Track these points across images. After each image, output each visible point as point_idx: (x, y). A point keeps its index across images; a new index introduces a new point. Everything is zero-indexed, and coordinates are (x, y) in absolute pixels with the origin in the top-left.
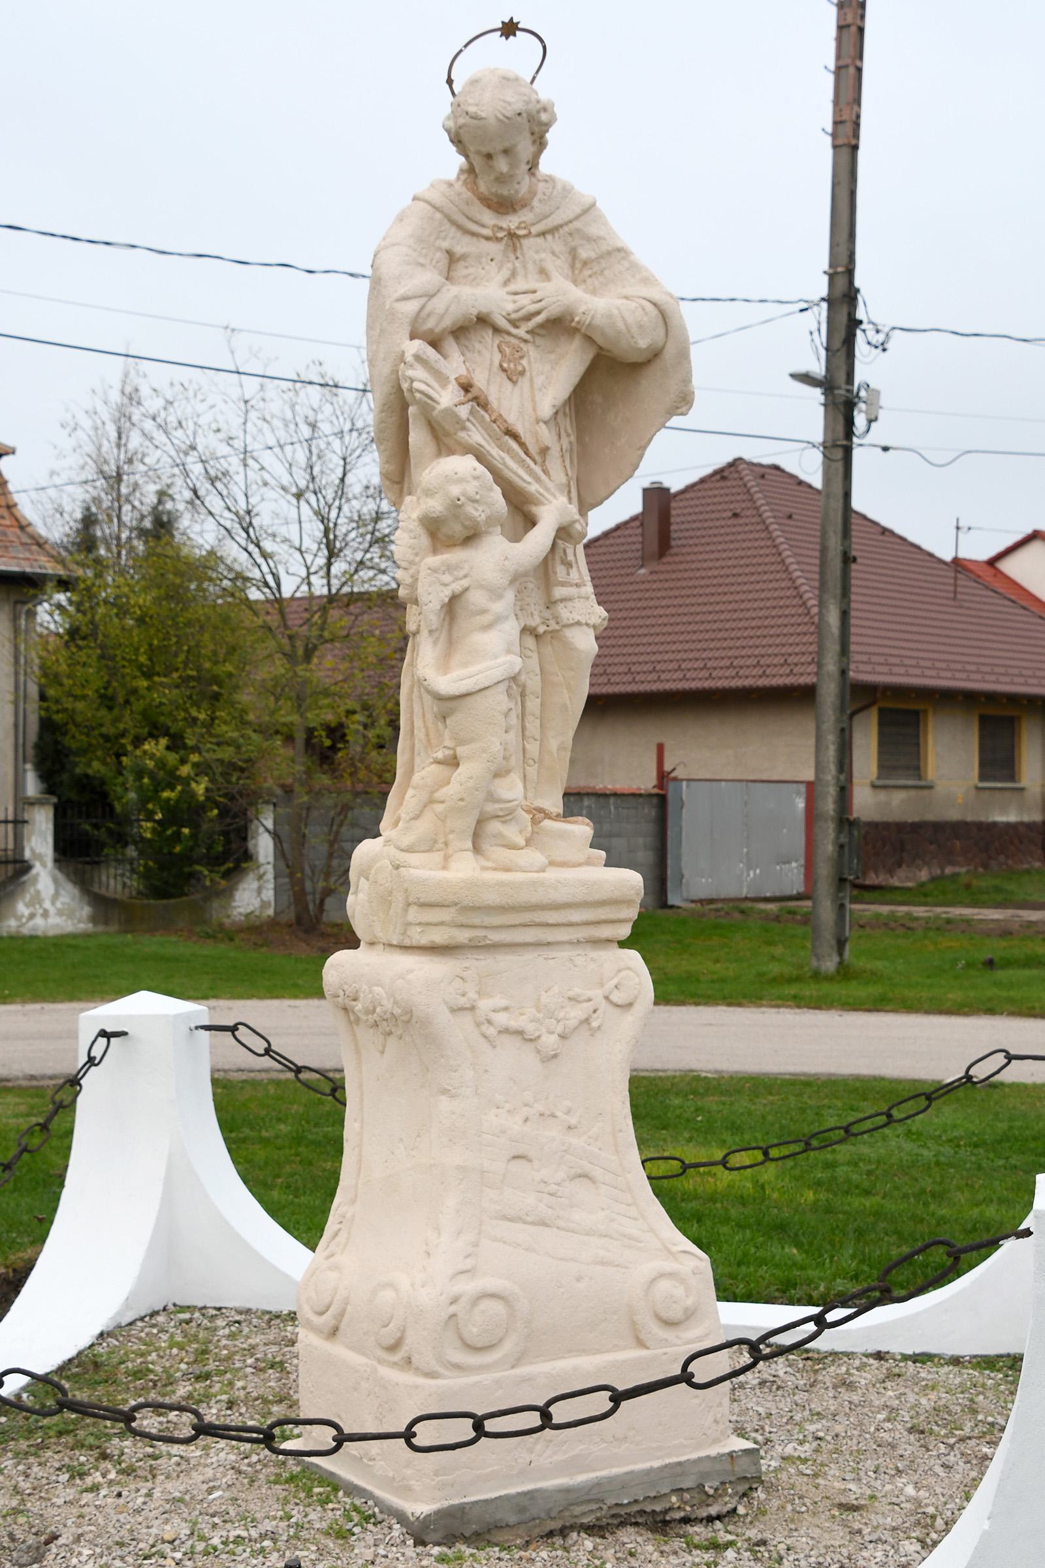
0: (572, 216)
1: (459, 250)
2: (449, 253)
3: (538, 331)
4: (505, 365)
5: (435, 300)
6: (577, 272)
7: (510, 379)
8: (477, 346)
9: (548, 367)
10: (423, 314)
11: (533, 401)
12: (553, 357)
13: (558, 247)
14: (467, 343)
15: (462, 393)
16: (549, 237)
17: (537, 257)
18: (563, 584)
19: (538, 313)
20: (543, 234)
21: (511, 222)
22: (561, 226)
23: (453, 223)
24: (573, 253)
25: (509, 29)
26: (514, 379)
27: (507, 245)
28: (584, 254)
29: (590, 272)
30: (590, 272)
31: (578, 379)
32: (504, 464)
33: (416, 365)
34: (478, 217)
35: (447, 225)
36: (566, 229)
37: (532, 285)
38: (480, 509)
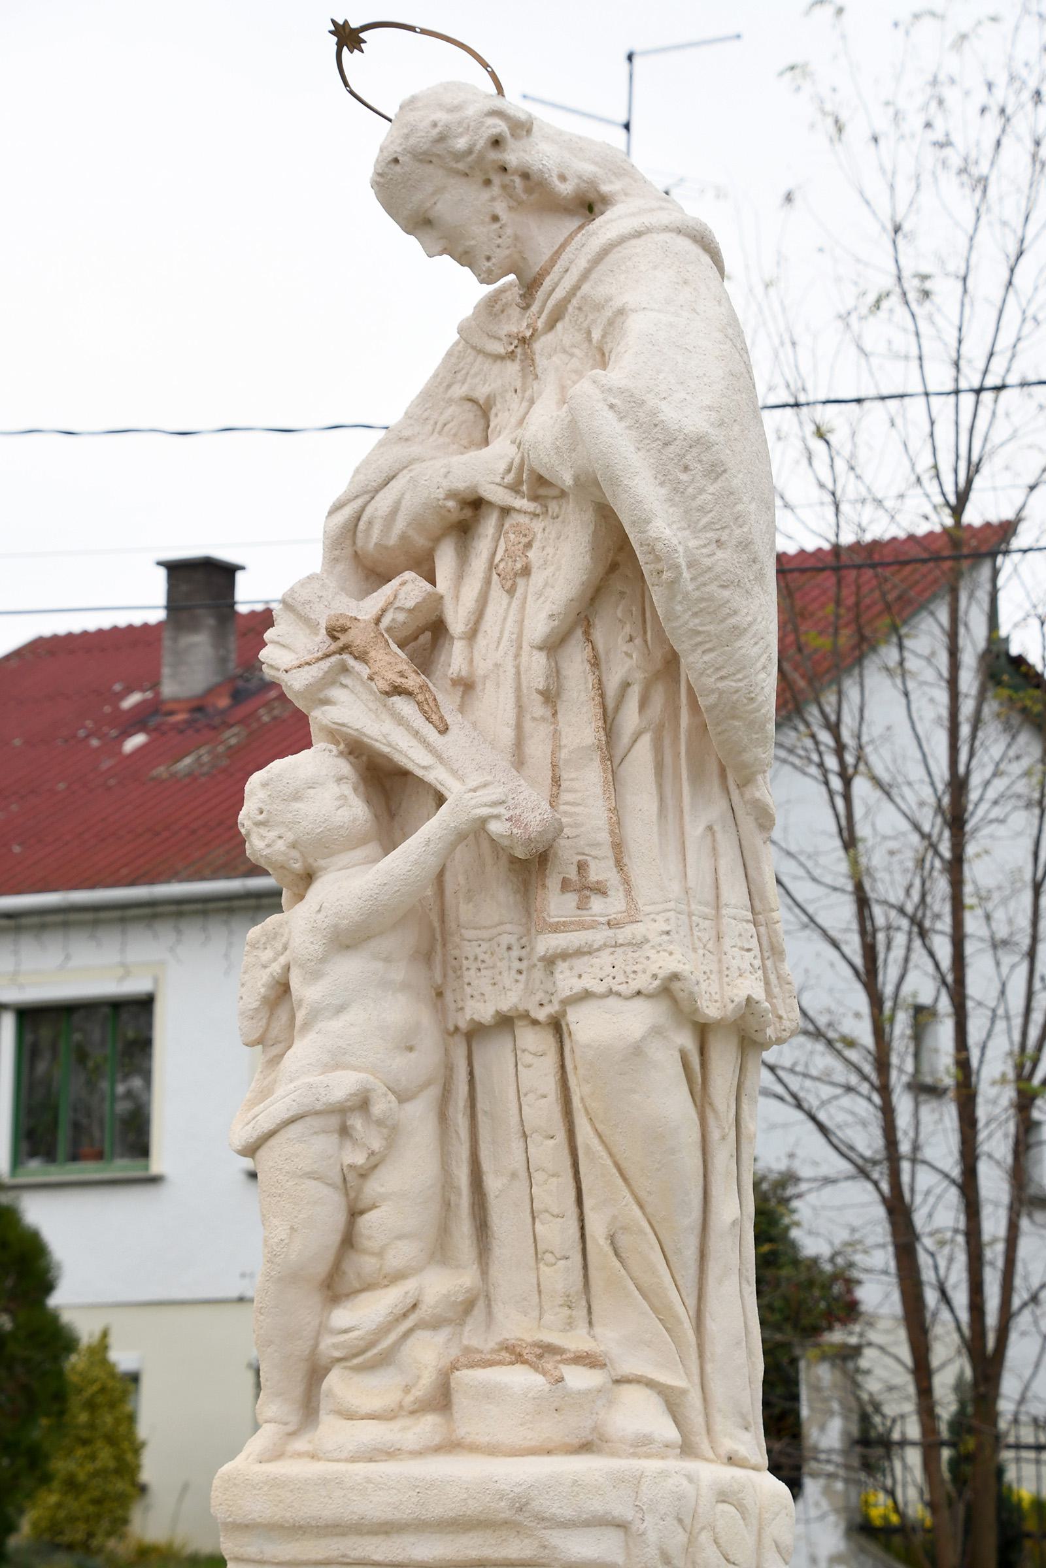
1: (481, 393)
10: (362, 526)
18: (556, 928)
22: (567, 300)
25: (348, 37)
32: (389, 745)
36: (574, 302)
38: (272, 834)
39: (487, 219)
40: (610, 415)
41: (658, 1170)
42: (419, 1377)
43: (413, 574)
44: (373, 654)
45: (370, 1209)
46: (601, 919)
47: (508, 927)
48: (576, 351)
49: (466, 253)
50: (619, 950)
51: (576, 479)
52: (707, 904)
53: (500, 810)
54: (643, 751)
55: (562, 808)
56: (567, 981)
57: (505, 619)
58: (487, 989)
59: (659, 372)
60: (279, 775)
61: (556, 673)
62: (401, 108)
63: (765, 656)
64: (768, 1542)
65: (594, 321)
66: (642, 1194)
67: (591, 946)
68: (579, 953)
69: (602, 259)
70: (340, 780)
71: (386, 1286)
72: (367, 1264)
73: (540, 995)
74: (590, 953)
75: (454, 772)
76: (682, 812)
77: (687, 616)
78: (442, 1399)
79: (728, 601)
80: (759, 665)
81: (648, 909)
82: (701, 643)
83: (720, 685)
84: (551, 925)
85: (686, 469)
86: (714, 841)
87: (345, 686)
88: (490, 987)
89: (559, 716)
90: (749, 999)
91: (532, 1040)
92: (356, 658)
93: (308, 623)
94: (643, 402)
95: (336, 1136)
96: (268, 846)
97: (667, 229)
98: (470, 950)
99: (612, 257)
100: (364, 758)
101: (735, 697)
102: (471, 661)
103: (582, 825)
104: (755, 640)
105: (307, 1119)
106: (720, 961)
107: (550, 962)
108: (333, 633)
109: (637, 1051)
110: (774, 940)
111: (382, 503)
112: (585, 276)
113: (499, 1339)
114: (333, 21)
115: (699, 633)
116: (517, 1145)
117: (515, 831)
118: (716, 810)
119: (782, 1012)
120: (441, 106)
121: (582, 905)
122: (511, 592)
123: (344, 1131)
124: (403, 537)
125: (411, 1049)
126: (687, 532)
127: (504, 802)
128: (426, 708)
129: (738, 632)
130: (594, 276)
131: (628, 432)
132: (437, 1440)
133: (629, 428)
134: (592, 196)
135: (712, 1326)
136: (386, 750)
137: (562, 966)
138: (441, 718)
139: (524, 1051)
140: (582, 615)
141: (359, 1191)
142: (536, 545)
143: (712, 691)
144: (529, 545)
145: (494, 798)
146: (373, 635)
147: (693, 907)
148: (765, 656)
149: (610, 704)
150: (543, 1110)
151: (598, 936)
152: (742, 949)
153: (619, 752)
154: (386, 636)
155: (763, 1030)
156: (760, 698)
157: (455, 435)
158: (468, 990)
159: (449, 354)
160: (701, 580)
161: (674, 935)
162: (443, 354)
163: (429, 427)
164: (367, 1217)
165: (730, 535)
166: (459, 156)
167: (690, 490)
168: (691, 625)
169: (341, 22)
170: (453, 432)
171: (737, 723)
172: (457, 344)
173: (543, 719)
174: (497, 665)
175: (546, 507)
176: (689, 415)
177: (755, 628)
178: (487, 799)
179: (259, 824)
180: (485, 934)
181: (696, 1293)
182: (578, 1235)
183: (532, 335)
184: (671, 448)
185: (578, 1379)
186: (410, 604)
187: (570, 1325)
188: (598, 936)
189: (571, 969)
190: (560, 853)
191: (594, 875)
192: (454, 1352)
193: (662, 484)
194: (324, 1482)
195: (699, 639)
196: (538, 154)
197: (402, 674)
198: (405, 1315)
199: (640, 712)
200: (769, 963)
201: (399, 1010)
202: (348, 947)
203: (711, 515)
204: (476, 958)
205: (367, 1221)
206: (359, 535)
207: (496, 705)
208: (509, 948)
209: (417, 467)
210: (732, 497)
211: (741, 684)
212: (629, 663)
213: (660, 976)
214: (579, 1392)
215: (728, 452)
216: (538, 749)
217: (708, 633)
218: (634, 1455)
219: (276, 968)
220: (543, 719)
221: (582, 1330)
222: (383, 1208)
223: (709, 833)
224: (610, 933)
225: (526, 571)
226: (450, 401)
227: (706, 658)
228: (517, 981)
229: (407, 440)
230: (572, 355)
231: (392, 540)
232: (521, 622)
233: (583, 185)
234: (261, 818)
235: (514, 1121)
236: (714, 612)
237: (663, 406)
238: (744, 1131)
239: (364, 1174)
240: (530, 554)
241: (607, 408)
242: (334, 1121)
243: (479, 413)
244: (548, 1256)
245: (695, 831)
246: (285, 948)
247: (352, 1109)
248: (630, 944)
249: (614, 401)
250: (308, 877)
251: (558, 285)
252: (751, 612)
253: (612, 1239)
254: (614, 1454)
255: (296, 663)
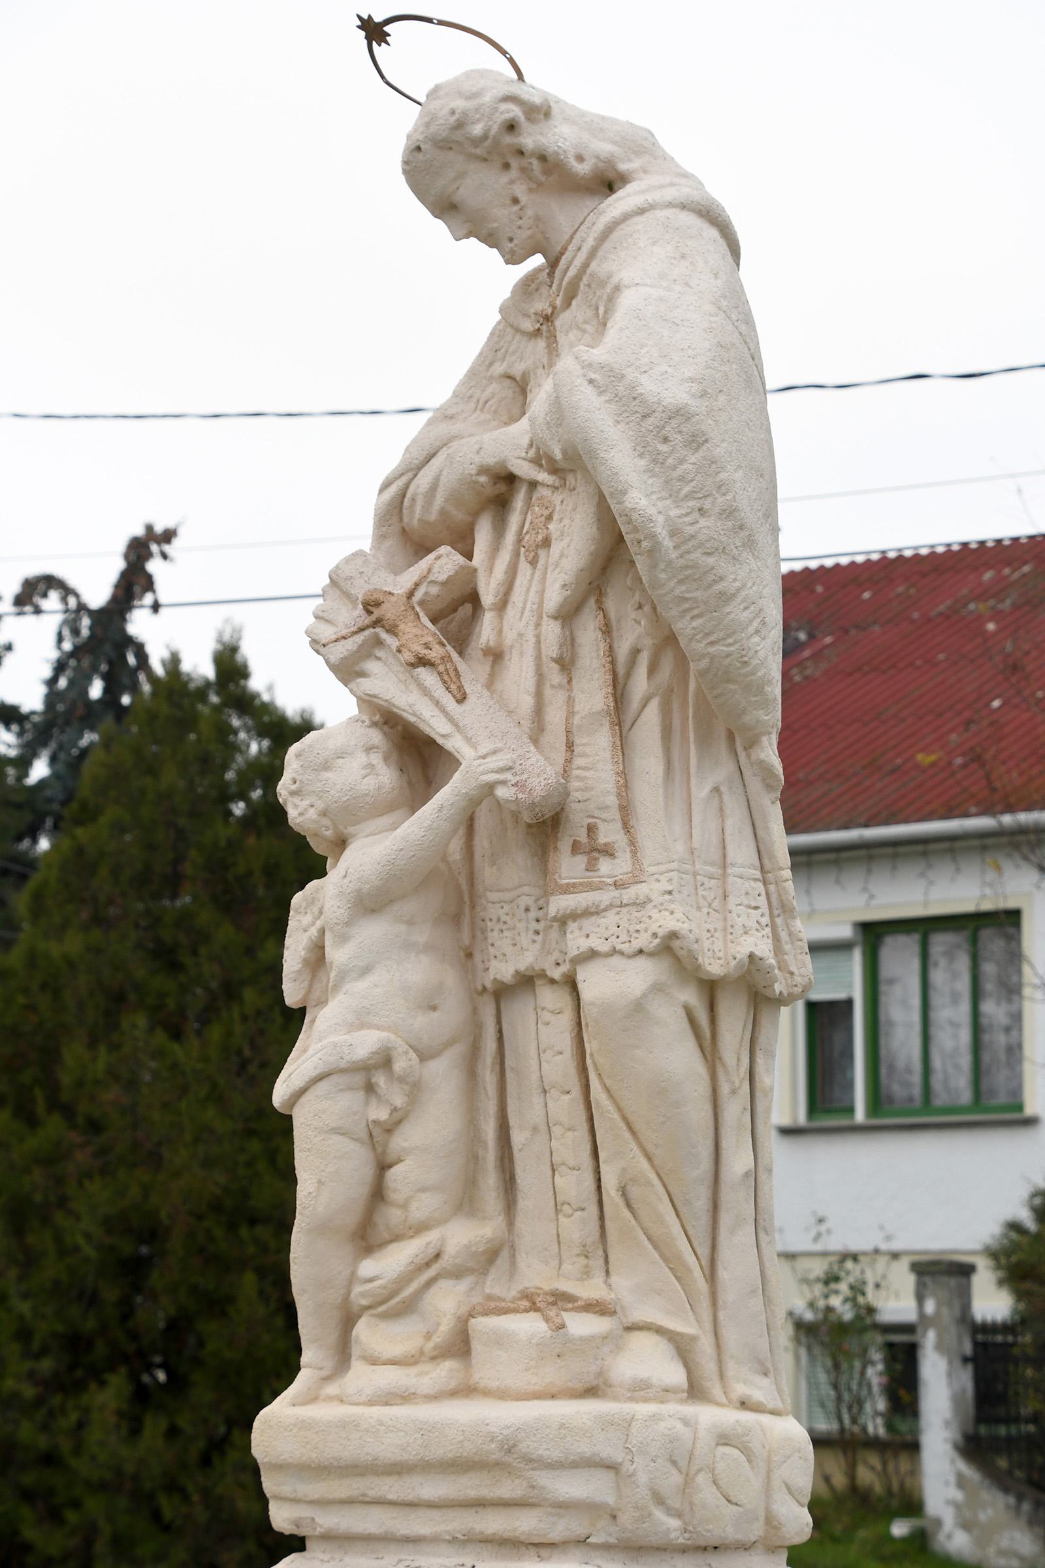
1: (518, 370)
18: (567, 890)
22: (578, 278)
25: (374, 32)
32: (415, 715)
36: (585, 280)
38: (305, 803)
39: (508, 202)
40: (589, 390)
41: (663, 1123)
42: (438, 1324)
43: (449, 548)
44: (402, 627)
45: (397, 1163)
46: (609, 880)
47: (526, 889)
48: (587, 327)
49: (491, 235)
50: (625, 910)
51: (564, 452)
52: (712, 864)
53: (508, 776)
54: (651, 718)
55: (576, 772)
56: (577, 941)
57: (528, 590)
58: (508, 949)
59: (642, 347)
60: (311, 746)
61: (570, 643)
62: (427, 96)
63: (758, 620)
64: (776, 1483)
65: (600, 298)
66: (650, 1148)
67: (598, 906)
68: (587, 913)
69: (607, 237)
70: (369, 749)
71: (412, 1237)
72: (392, 1216)
73: (556, 955)
74: (597, 913)
75: (468, 740)
76: (689, 773)
77: (672, 584)
78: (460, 1346)
79: (713, 568)
80: (751, 629)
81: (652, 869)
82: (687, 610)
83: (711, 650)
84: (561, 887)
85: (666, 440)
86: (721, 802)
87: (379, 659)
88: (511, 948)
89: (574, 682)
90: (751, 956)
91: (551, 998)
92: (388, 631)
93: (348, 596)
94: (623, 376)
95: (362, 1093)
96: (301, 814)
97: (670, 205)
98: (493, 912)
99: (615, 236)
100: (399, 728)
101: (727, 661)
102: (500, 631)
103: (592, 789)
104: (745, 604)
105: (334, 1076)
106: (725, 919)
107: (563, 921)
108: (370, 606)
109: (638, 1007)
110: (784, 898)
111: (423, 480)
112: (592, 254)
113: (521, 1287)
114: (358, 16)
115: (687, 599)
116: (537, 1100)
117: (520, 796)
118: (723, 771)
119: (793, 968)
120: (460, 94)
121: (591, 867)
122: (533, 563)
123: (370, 1089)
124: (443, 512)
125: (434, 1008)
126: (668, 502)
127: (511, 768)
128: (446, 678)
129: (726, 598)
130: (600, 253)
131: (607, 405)
132: (453, 1384)
133: (609, 401)
134: (611, 175)
135: (723, 1274)
136: (412, 719)
137: (572, 926)
138: (461, 687)
139: (543, 1009)
140: (595, 584)
141: (386, 1145)
142: (556, 517)
143: (703, 656)
144: (549, 518)
145: (501, 764)
146: (403, 608)
147: (698, 866)
148: (758, 620)
149: (621, 671)
150: (559, 1065)
151: (604, 897)
152: (749, 907)
153: (628, 718)
154: (418, 609)
155: (772, 986)
156: (755, 662)
157: (495, 412)
158: (492, 950)
159: (492, 334)
160: (684, 548)
161: (676, 895)
162: (488, 335)
163: (473, 405)
164: (393, 1170)
165: (713, 503)
166: (477, 142)
167: (670, 461)
168: (677, 592)
169: (366, 17)
170: (493, 408)
171: (732, 687)
172: (499, 323)
173: (560, 686)
174: (520, 635)
175: (565, 479)
176: (668, 386)
177: (744, 593)
178: (493, 766)
179: (293, 793)
180: (507, 896)
181: (709, 1243)
182: (593, 1187)
183: (552, 313)
184: (650, 420)
185: (581, 1325)
186: (443, 577)
187: (587, 1273)
188: (604, 897)
189: (580, 929)
190: (571, 817)
191: (602, 839)
192: (476, 1299)
193: (641, 456)
194: (346, 1425)
195: (687, 606)
196: (559, 137)
197: (427, 646)
198: (428, 1265)
199: (649, 678)
200: (779, 921)
201: (419, 971)
202: (373, 911)
203: (692, 484)
204: (499, 920)
205: (395, 1174)
206: (405, 511)
207: (519, 675)
208: (527, 910)
209: (455, 444)
210: (714, 466)
211: (732, 648)
212: (639, 630)
213: (660, 935)
214: (581, 1338)
215: (710, 421)
216: (555, 716)
217: (695, 600)
218: (631, 1399)
219: (313, 931)
220: (560, 686)
221: (598, 1279)
222: (407, 1162)
223: (716, 795)
224: (616, 893)
225: (546, 543)
226: (491, 379)
227: (695, 624)
228: (534, 941)
229: (452, 418)
230: (584, 331)
231: (433, 516)
232: (542, 593)
233: (601, 165)
234: (294, 787)
235: (535, 1077)
236: (700, 579)
237: (643, 379)
238: (758, 1085)
239: (390, 1129)
240: (551, 527)
241: (586, 383)
242: (359, 1079)
243: (517, 390)
244: (566, 1207)
245: (701, 791)
246: (321, 913)
247: (376, 1067)
248: (634, 904)
249: (593, 376)
250: (342, 843)
251: (572, 263)
252: (739, 577)
253: (624, 1192)
254: (615, 1398)
255: (334, 637)
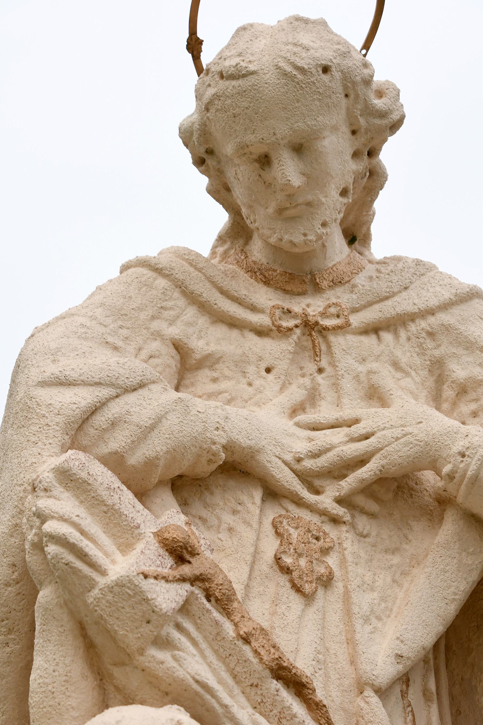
0: (434, 302)
2: (179, 347)
3: (361, 500)
4: (288, 560)
5: (131, 398)
6: (445, 406)
7: (298, 590)
8: (228, 519)
9: (383, 579)
10: (100, 420)
11: (351, 642)
12: (396, 559)
13: (405, 354)
14: (204, 513)
15: (169, 561)
16: (387, 337)
17: (362, 369)
19: (362, 461)
20: (374, 330)
21: (313, 306)
22: (412, 317)
23: (193, 299)
24: (438, 370)
26: (307, 588)
27: (300, 347)
28: (460, 370)
29: (473, 406)
30: (473, 406)
31: (451, 610)
33: (58, 490)
34: (243, 292)
35: (181, 302)
36: (423, 324)
37: (347, 413)
111: (140, 408)
124: (150, 464)
166: (371, 112)
231: (135, 459)
